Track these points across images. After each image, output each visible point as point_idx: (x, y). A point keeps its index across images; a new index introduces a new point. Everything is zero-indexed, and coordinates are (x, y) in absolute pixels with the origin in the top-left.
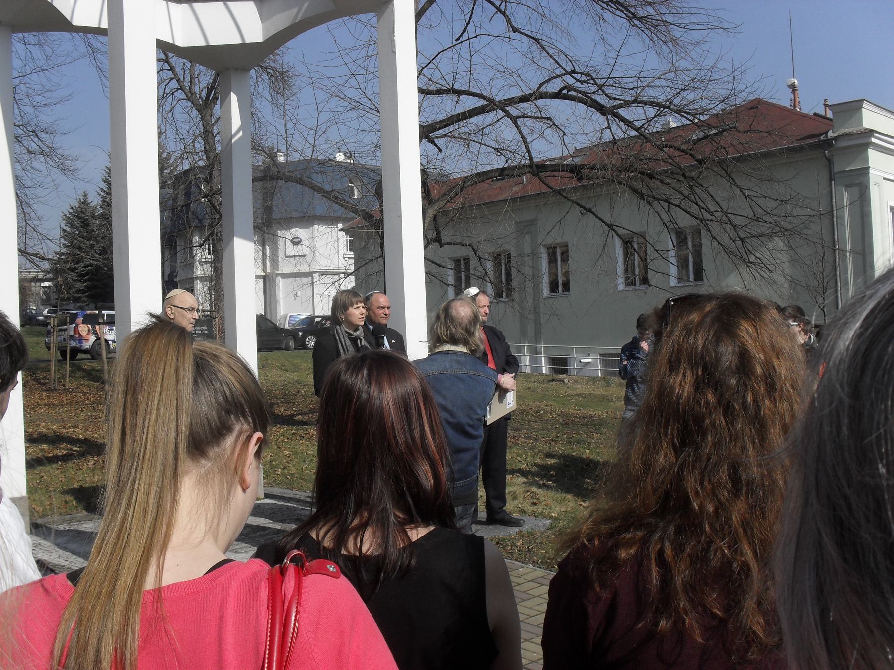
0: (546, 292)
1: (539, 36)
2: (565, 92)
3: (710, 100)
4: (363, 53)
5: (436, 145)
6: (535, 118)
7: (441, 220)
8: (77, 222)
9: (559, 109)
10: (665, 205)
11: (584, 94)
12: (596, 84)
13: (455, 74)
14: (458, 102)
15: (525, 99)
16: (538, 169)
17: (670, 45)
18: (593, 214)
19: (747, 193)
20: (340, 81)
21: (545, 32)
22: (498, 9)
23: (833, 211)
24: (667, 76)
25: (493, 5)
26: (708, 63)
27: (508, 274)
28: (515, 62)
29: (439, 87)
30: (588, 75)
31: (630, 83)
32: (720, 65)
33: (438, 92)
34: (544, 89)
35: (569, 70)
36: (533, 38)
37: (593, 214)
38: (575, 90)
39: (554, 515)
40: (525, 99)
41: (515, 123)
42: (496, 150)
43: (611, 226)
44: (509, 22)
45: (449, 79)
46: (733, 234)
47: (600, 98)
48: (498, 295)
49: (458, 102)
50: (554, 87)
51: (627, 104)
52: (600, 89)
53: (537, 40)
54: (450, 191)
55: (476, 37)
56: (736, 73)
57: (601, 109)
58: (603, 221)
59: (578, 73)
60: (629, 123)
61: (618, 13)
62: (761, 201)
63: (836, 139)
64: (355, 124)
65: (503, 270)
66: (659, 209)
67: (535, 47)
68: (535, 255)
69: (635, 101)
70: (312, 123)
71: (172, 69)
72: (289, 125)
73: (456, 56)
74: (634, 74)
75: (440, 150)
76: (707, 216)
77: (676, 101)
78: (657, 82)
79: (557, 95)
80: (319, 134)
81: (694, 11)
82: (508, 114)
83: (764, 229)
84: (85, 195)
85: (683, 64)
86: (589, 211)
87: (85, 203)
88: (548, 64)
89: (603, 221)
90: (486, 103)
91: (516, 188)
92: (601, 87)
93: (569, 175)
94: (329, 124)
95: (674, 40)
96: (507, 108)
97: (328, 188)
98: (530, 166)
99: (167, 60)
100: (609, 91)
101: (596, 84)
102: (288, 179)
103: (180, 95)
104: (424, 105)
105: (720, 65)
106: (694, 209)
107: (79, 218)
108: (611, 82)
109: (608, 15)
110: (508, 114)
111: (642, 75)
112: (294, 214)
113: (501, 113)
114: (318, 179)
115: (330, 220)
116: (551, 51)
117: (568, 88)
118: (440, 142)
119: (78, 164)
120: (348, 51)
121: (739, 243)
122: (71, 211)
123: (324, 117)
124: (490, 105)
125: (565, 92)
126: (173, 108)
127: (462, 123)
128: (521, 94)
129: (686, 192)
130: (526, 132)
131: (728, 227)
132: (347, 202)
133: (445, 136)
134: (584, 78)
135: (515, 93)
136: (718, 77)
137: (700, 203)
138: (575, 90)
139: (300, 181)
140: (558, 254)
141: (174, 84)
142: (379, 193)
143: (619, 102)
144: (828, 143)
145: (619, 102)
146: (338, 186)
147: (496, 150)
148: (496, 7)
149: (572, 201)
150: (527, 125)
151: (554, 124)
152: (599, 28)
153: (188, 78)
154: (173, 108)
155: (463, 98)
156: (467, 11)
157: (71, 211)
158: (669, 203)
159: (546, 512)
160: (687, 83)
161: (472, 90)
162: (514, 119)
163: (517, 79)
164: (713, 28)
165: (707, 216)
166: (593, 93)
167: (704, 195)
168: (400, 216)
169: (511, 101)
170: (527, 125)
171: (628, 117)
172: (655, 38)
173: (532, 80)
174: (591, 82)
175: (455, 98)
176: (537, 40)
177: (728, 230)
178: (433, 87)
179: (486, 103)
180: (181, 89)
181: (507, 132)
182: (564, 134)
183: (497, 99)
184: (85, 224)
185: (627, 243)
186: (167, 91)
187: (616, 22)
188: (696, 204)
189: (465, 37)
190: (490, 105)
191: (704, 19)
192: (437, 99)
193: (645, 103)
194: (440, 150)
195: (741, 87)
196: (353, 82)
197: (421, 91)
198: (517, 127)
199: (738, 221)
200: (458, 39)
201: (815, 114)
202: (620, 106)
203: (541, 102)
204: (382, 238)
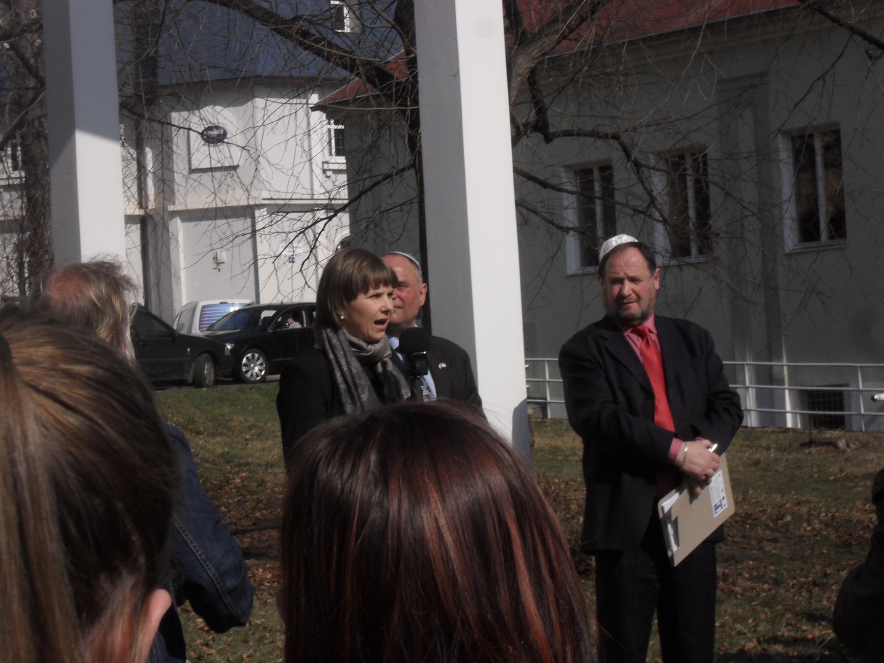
0: (790, 237)
27: (703, 202)
48: (681, 249)
54: (568, 10)
68: (764, 155)
112: (210, 75)
115: (290, 85)
132: (330, 45)
140: (818, 151)
149: (851, 29)
168: (456, 75)
204: (415, 123)
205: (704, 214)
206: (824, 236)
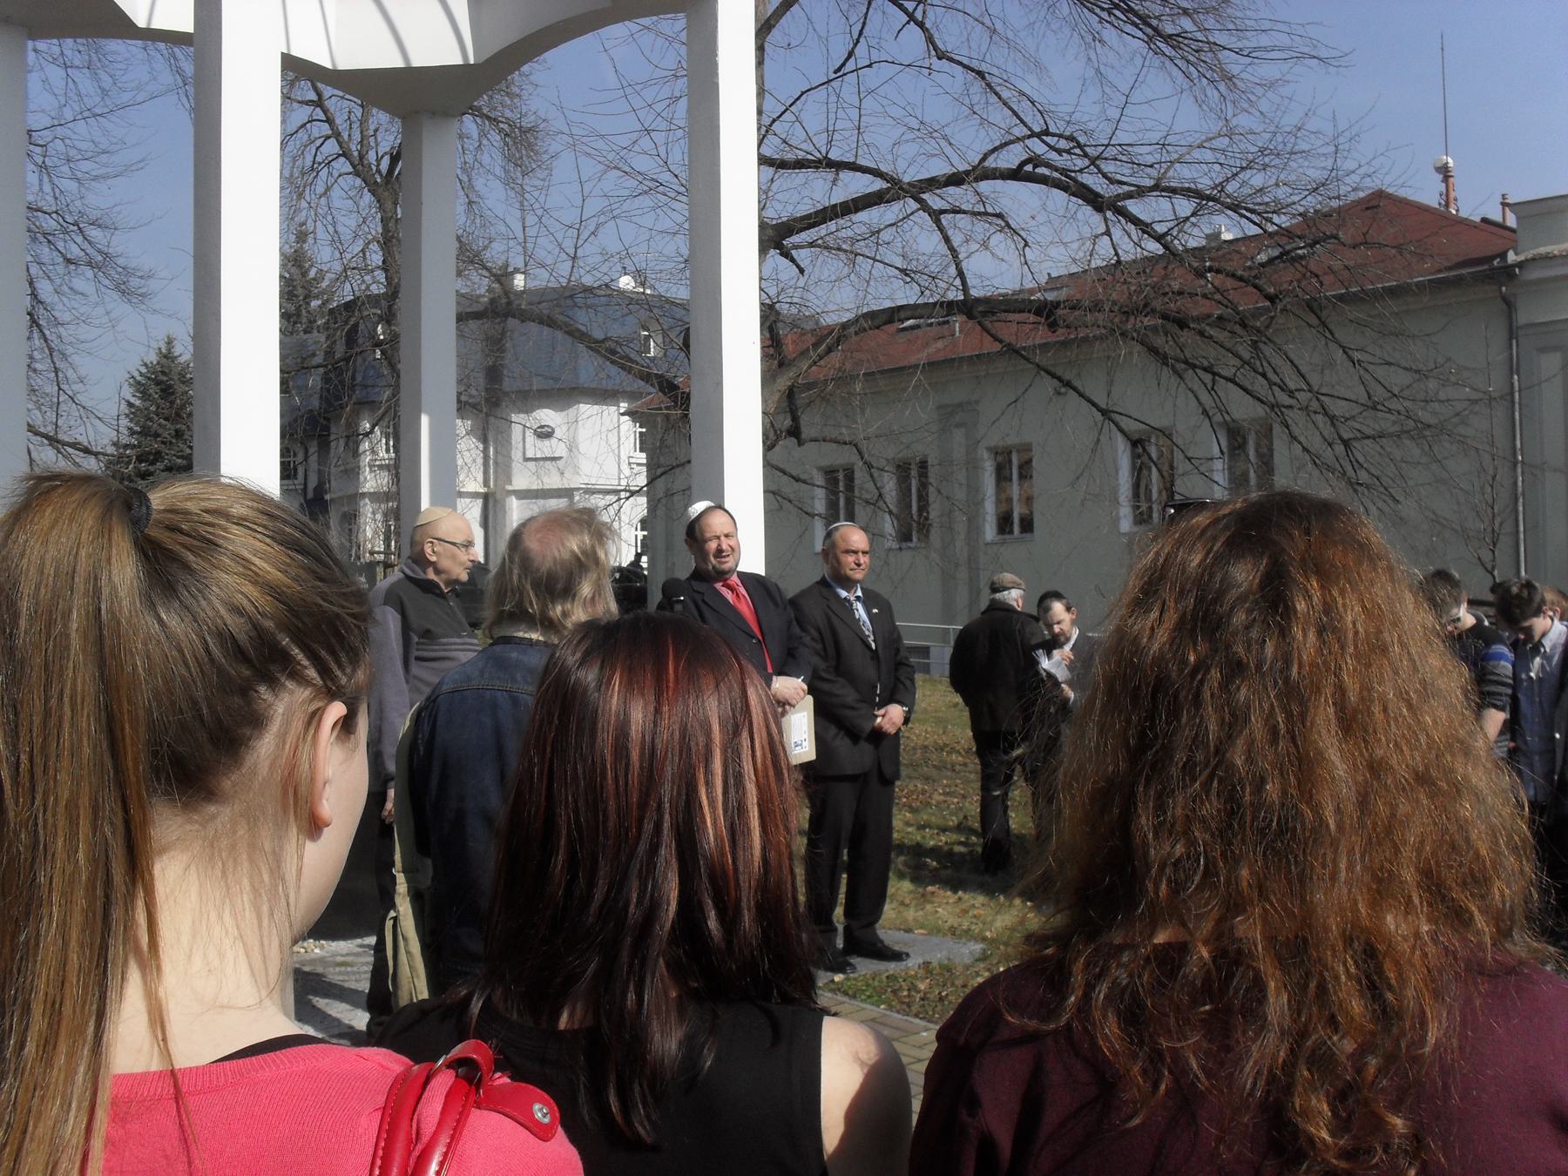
0: (990, 532)
1: (984, 67)
2: (1029, 168)
3: (1294, 189)
4: (666, 92)
5: (793, 260)
6: (975, 214)
7: (802, 398)
8: (154, 391)
9: (1018, 199)
10: (1208, 378)
11: (1064, 172)
12: (1086, 155)
13: (830, 133)
14: (834, 182)
15: (956, 180)
16: (976, 310)
17: (1222, 87)
18: (1075, 389)
19: (1357, 356)
20: (624, 141)
21: (998, 61)
22: (911, 17)
23: (1512, 394)
24: (1217, 143)
25: (901, 7)
26: (1289, 121)
28: (939, 111)
29: (801, 155)
30: (1071, 138)
31: (1146, 155)
32: (1313, 124)
33: (800, 164)
34: (991, 163)
35: (1037, 129)
36: (973, 70)
37: (1075, 389)
38: (1048, 165)
39: (988, 934)
40: (956, 180)
41: (938, 222)
42: (903, 271)
43: (1105, 413)
44: (930, 40)
45: (821, 141)
46: (1328, 431)
47: (1092, 180)
48: (905, 537)
49: (834, 182)
50: (1010, 158)
51: (1140, 192)
52: (1093, 163)
53: (980, 74)
54: (816, 345)
55: (870, 66)
56: (1341, 140)
57: (1096, 202)
58: (1094, 404)
59: (1054, 135)
60: (1145, 227)
61: (1129, 28)
62: (1380, 372)
63: (1520, 265)
64: (648, 221)
65: (914, 490)
66: (1196, 385)
67: (978, 85)
68: (973, 466)
69: (1156, 187)
70: (571, 216)
71: (329, 121)
72: (531, 220)
73: (833, 98)
74: (1155, 137)
75: (802, 271)
76: (1284, 399)
77: (1230, 188)
78: (1197, 154)
79: (1016, 174)
80: (583, 236)
81: (1267, 25)
82: (924, 207)
83: (1386, 422)
84: (170, 342)
85: (1243, 121)
86: (1068, 384)
87: (168, 356)
88: (1000, 116)
89: (1094, 404)
90: (885, 185)
91: (940, 345)
92: (1093, 161)
93: (1032, 318)
94: (602, 219)
95: (1229, 78)
96: (924, 196)
97: (598, 334)
98: (964, 302)
99: (319, 103)
100: (1108, 167)
101: (1086, 155)
102: (524, 317)
103: (342, 165)
104: (775, 187)
105: (1313, 124)
106: (1260, 385)
107: (158, 383)
108: (1111, 152)
109: (1109, 34)
110: (924, 207)
111: (1170, 139)
113: (912, 205)
114: (582, 319)
115: (604, 395)
116: (1005, 94)
117: (1035, 160)
118: (802, 255)
119: (153, 285)
120: (638, 88)
121: (1340, 449)
122: (144, 370)
123: (593, 206)
124: (894, 190)
125: (1029, 168)
126: (328, 189)
127: (841, 221)
128: (948, 170)
129: (1246, 355)
130: (957, 240)
131: (1320, 418)
133: (811, 245)
134: (1063, 144)
135: (939, 169)
136: (1305, 147)
137: (1271, 375)
138: (1048, 165)
139: (550, 322)
140: (1013, 465)
141: (331, 147)
142: (686, 345)
143: (1126, 188)
144: (1508, 273)
145: (1126, 188)
146: (616, 331)
147: (903, 271)
148: (905, 11)
150: (959, 227)
151: (1009, 226)
152: (1093, 57)
153: (357, 136)
154: (328, 189)
155: (845, 175)
156: (855, 17)
157: (144, 370)
158: (1214, 374)
159: (976, 929)
160: (1250, 157)
161: (862, 162)
162: (936, 215)
163: (943, 143)
164: (1302, 56)
165: (1284, 399)
166: (1081, 171)
167: (1278, 361)
168: (719, 384)
169: (932, 183)
170: (959, 227)
171: (1142, 217)
172: (1195, 74)
173: (971, 145)
174: (1078, 151)
175: (829, 175)
176: (980, 74)
177: (1321, 425)
178: (790, 156)
179: (885, 185)
180: (344, 155)
181: (924, 241)
182: (1026, 244)
183: (906, 179)
184: (167, 391)
185: (1137, 443)
186: (319, 159)
187: (1123, 46)
188: (1264, 375)
189: (850, 66)
190: (894, 190)
191: (1284, 40)
192: (800, 176)
193: (1174, 191)
194: (802, 271)
195: (1350, 165)
196: (645, 143)
197: (764, 161)
198: (941, 229)
199: (1338, 408)
200: (839, 69)
201: (1484, 220)
202: (1129, 196)
203: (985, 186)
205: (924, 506)
206: (1016, 529)
